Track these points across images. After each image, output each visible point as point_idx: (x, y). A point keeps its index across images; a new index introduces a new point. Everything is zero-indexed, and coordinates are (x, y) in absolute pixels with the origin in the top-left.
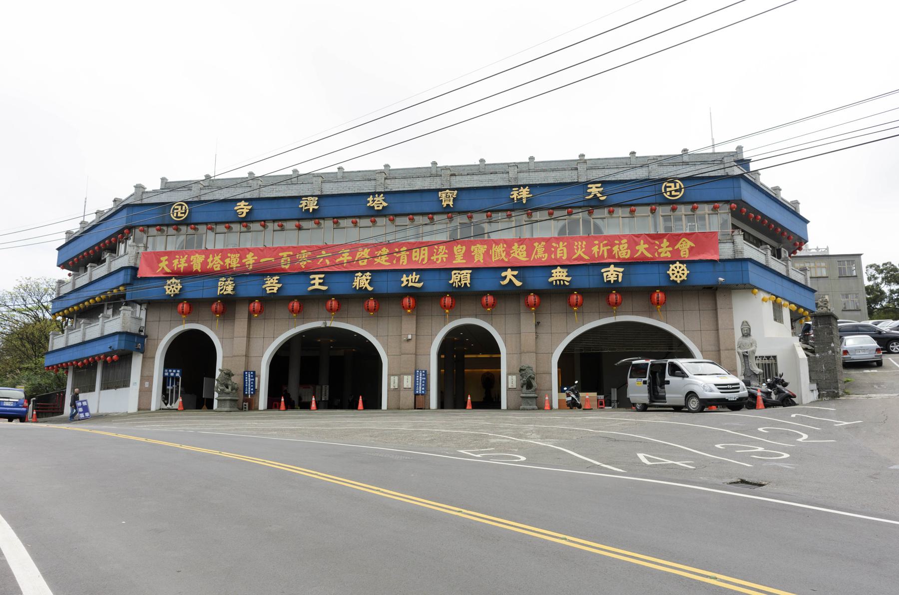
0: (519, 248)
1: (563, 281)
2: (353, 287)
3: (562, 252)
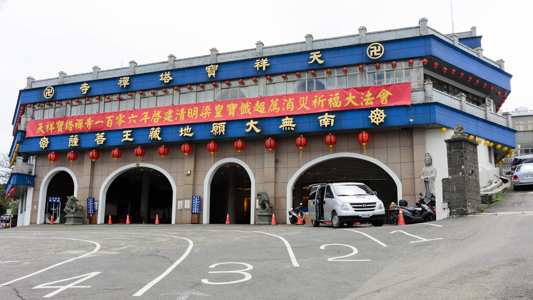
0: (260, 104)
1: (290, 127)
2: (149, 138)
3: (290, 105)
